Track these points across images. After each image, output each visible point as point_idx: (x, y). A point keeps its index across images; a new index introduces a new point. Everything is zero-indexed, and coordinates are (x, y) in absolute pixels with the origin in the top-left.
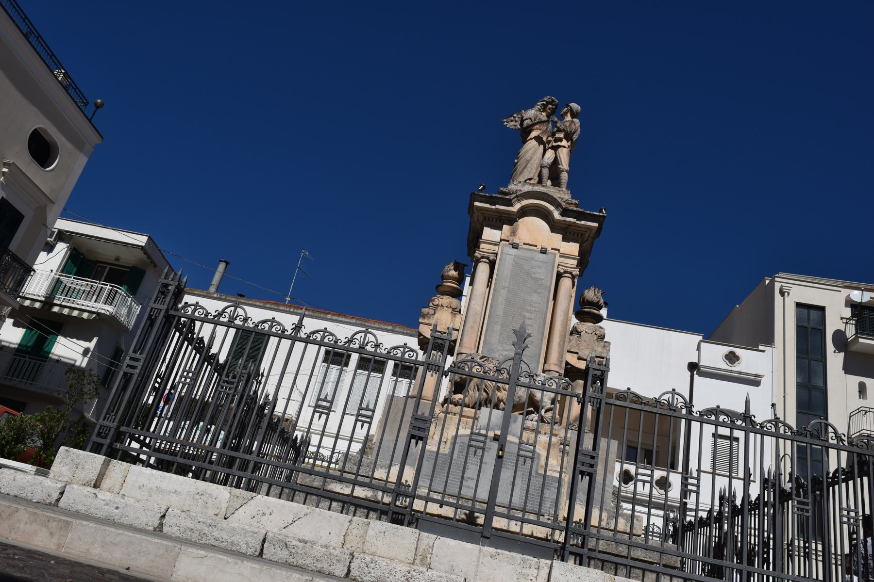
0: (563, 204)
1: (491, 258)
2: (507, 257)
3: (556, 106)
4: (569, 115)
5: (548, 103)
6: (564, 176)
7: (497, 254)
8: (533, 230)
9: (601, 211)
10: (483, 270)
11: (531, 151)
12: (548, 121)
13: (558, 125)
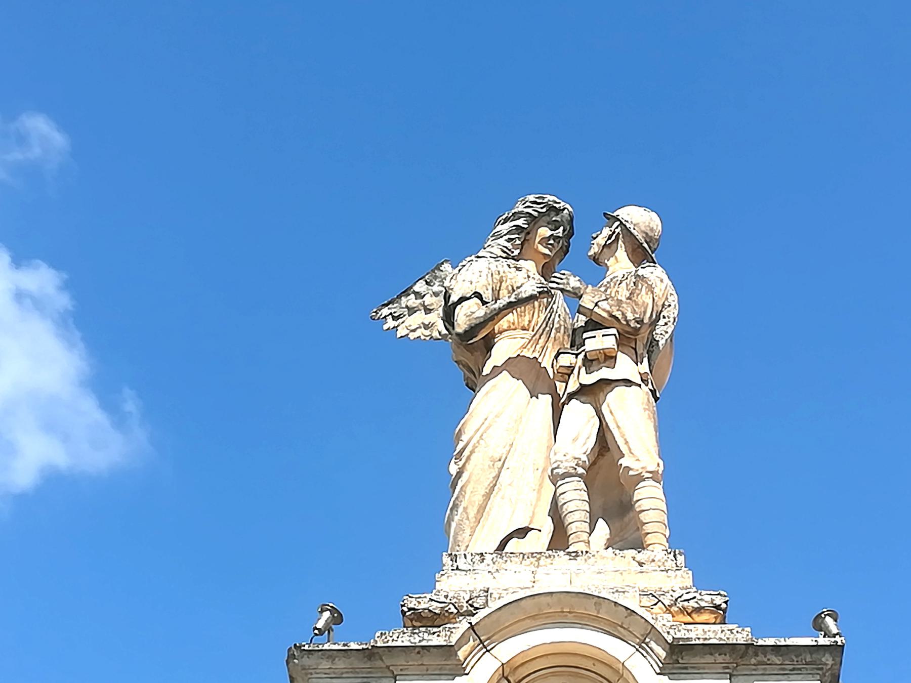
0: (663, 622)
4: (621, 253)
5: (533, 220)
6: (650, 500)
9: (818, 625)
12: (545, 293)
13: (587, 302)
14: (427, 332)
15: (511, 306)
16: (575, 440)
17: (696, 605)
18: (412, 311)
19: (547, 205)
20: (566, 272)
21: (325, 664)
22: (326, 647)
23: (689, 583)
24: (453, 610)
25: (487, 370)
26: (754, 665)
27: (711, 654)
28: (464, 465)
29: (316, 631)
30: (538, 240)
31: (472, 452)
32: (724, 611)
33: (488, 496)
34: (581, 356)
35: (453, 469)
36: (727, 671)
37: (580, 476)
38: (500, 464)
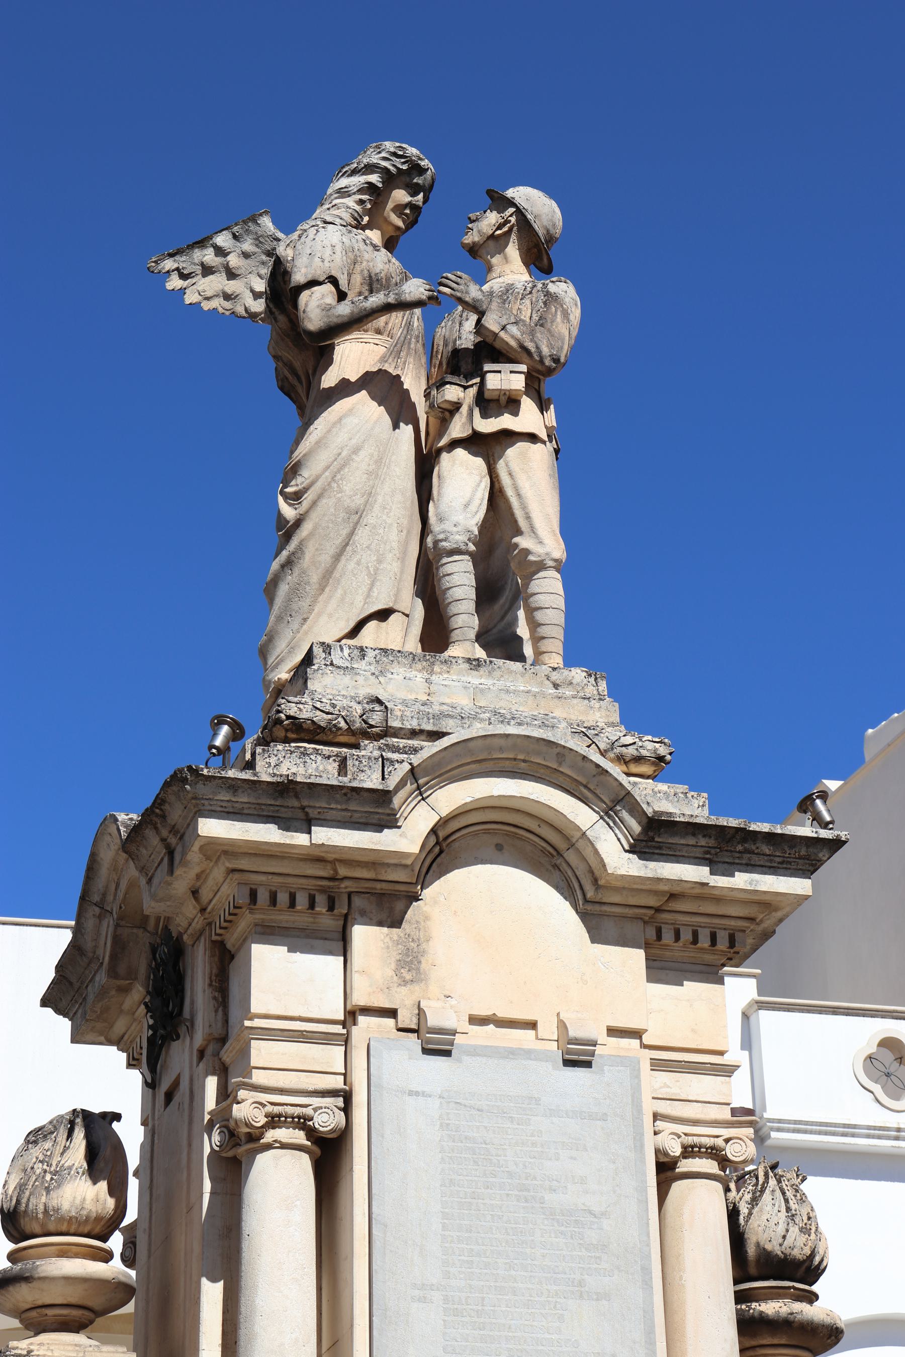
1: (327, 1119)
2: (408, 1119)
3: (427, 191)
4: (513, 250)
5: (391, 179)
7: (348, 1097)
8: (496, 932)
10: (280, 1186)
11: (363, 461)
13: (492, 322)
14: (228, 305)
15: (387, 308)
16: (467, 506)
17: (635, 753)
18: (207, 270)
19: (408, 160)
20: (464, 276)
21: (224, 796)
22: (231, 773)
23: (616, 718)
24: (342, 724)
25: (329, 380)
26: (740, 852)
27: (694, 835)
28: (307, 512)
29: (214, 751)
30: (390, 205)
31: (320, 497)
32: (667, 763)
33: (337, 557)
34: (472, 392)
35: (288, 512)
36: (708, 856)
37: (470, 554)
38: (356, 517)
